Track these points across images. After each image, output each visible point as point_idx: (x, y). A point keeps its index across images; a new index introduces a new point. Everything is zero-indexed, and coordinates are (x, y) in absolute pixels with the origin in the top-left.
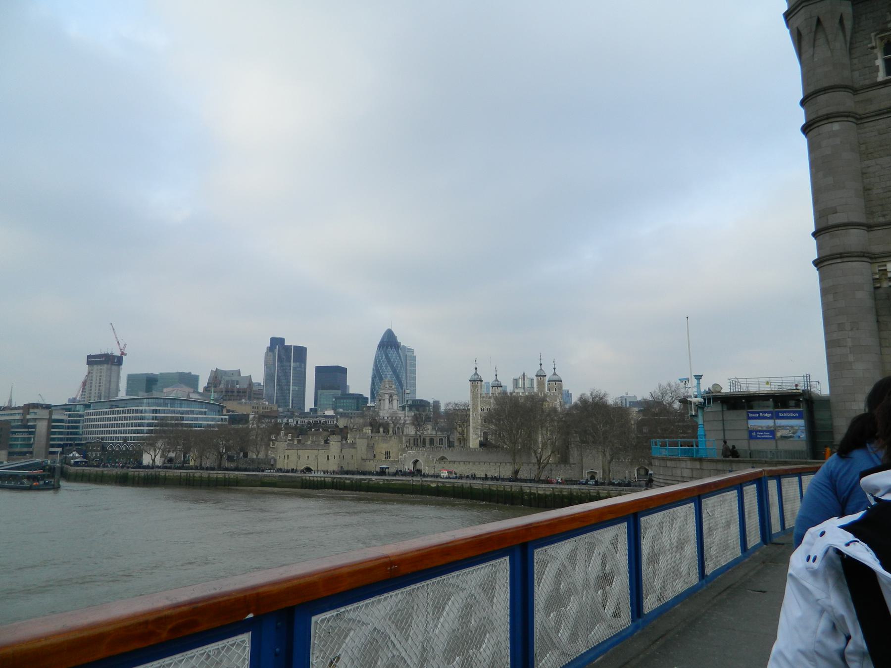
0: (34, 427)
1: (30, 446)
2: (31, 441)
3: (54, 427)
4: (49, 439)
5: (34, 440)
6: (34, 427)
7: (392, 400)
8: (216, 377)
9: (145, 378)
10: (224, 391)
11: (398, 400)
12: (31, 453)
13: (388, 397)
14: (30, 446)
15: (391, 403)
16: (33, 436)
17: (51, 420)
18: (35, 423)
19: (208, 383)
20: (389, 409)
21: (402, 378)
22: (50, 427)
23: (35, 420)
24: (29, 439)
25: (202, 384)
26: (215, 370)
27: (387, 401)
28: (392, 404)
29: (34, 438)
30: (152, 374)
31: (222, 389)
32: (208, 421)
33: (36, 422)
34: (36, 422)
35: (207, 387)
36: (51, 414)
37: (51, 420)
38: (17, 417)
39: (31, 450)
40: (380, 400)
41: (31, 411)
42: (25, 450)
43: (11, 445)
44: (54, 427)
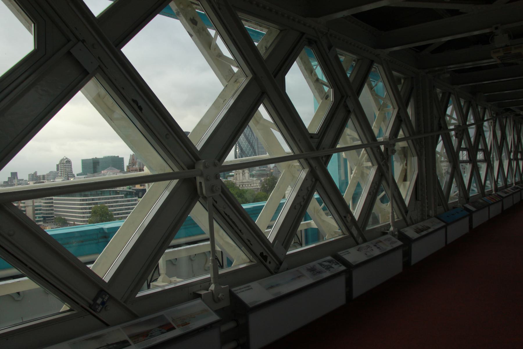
3: (37, 210)
7: (245, 173)
8: (133, 159)
9: (92, 162)
10: (138, 169)
11: (248, 173)
13: (242, 172)
15: (244, 175)
17: (34, 206)
19: (129, 163)
20: (243, 179)
21: (255, 146)
23: (25, 207)
25: (126, 163)
26: (132, 154)
27: (241, 174)
28: (245, 176)
30: (96, 158)
31: (137, 168)
32: (123, 210)
33: (25, 208)
34: (25, 208)
35: (129, 166)
37: (34, 206)
40: (236, 174)
44: (37, 210)
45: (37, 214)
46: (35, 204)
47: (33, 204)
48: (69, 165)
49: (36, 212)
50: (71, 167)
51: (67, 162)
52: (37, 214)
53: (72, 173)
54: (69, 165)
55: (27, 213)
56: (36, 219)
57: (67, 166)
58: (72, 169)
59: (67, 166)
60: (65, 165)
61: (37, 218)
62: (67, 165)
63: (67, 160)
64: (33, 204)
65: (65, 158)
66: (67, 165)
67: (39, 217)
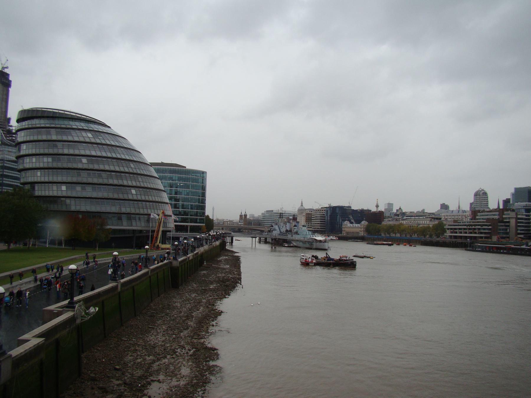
0: (509, 222)
1: (507, 233)
2: (507, 230)
4: (517, 230)
5: (509, 230)
6: (509, 222)
12: (508, 238)
14: (507, 233)
16: (508, 228)
17: (517, 219)
18: (509, 220)
22: (517, 222)
23: (509, 218)
24: (506, 229)
29: (509, 229)
36: (517, 214)
37: (517, 219)
38: (497, 217)
39: (508, 236)
41: (505, 213)
42: (504, 236)
43: (499, 232)
45: (519, 226)
46: (519, 216)
47: (517, 216)
48: (485, 197)
49: (518, 224)
50: (487, 199)
51: (483, 193)
52: (519, 226)
53: (488, 205)
54: (485, 197)
55: (511, 224)
56: (519, 232)
57: (483, 198)
58: (488, 201)
59: (483, 198)
60: (481, 196)
61: (519, 230)
62: (484, 197)
63: (483, 191)
64: (517, 216)
65: (480, 190)
66: (484, 197)
67: (521, 230)
